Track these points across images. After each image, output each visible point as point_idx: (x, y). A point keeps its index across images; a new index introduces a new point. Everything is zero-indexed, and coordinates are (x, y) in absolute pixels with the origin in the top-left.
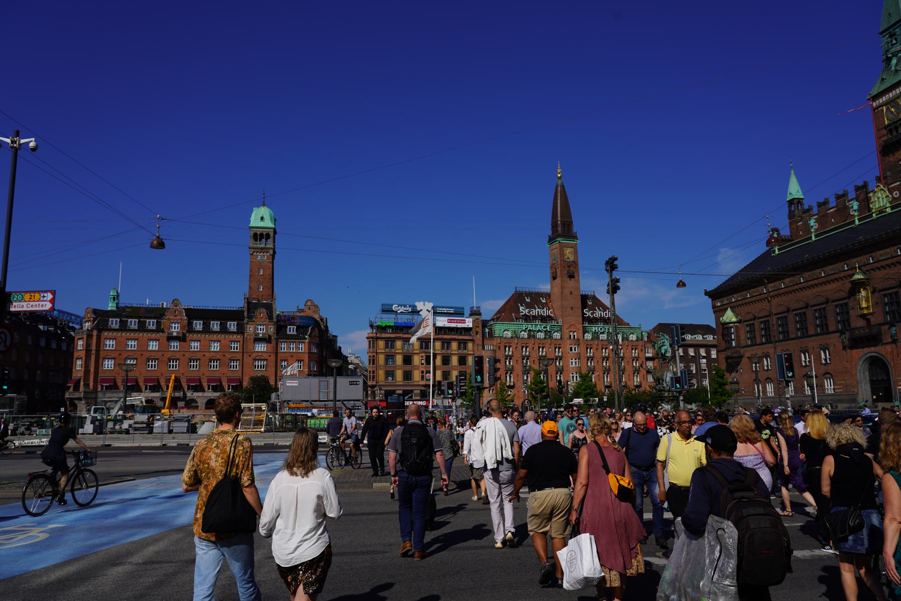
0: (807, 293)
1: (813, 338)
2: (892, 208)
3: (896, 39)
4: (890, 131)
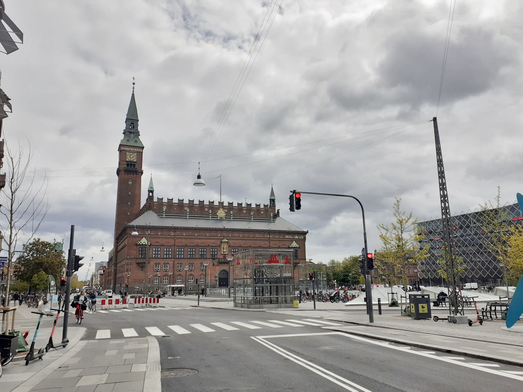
0: (199, 240)
1: (198, 259)
2: (225, 218)
3: (133, 126)
4: (128, 165)
